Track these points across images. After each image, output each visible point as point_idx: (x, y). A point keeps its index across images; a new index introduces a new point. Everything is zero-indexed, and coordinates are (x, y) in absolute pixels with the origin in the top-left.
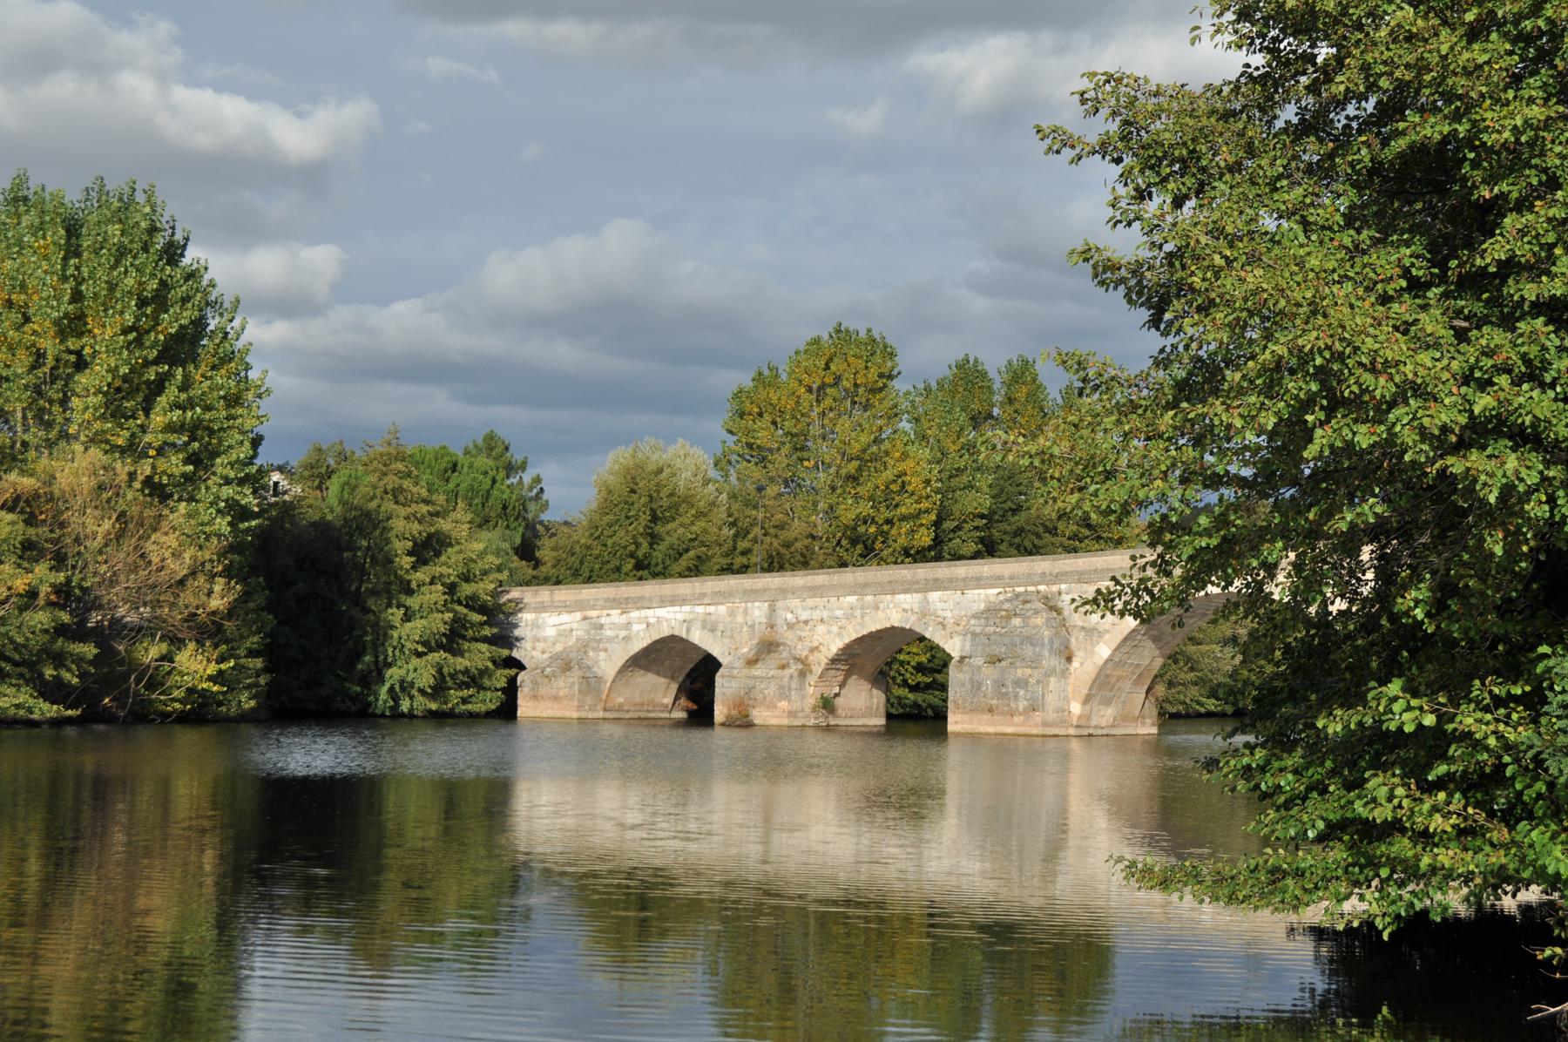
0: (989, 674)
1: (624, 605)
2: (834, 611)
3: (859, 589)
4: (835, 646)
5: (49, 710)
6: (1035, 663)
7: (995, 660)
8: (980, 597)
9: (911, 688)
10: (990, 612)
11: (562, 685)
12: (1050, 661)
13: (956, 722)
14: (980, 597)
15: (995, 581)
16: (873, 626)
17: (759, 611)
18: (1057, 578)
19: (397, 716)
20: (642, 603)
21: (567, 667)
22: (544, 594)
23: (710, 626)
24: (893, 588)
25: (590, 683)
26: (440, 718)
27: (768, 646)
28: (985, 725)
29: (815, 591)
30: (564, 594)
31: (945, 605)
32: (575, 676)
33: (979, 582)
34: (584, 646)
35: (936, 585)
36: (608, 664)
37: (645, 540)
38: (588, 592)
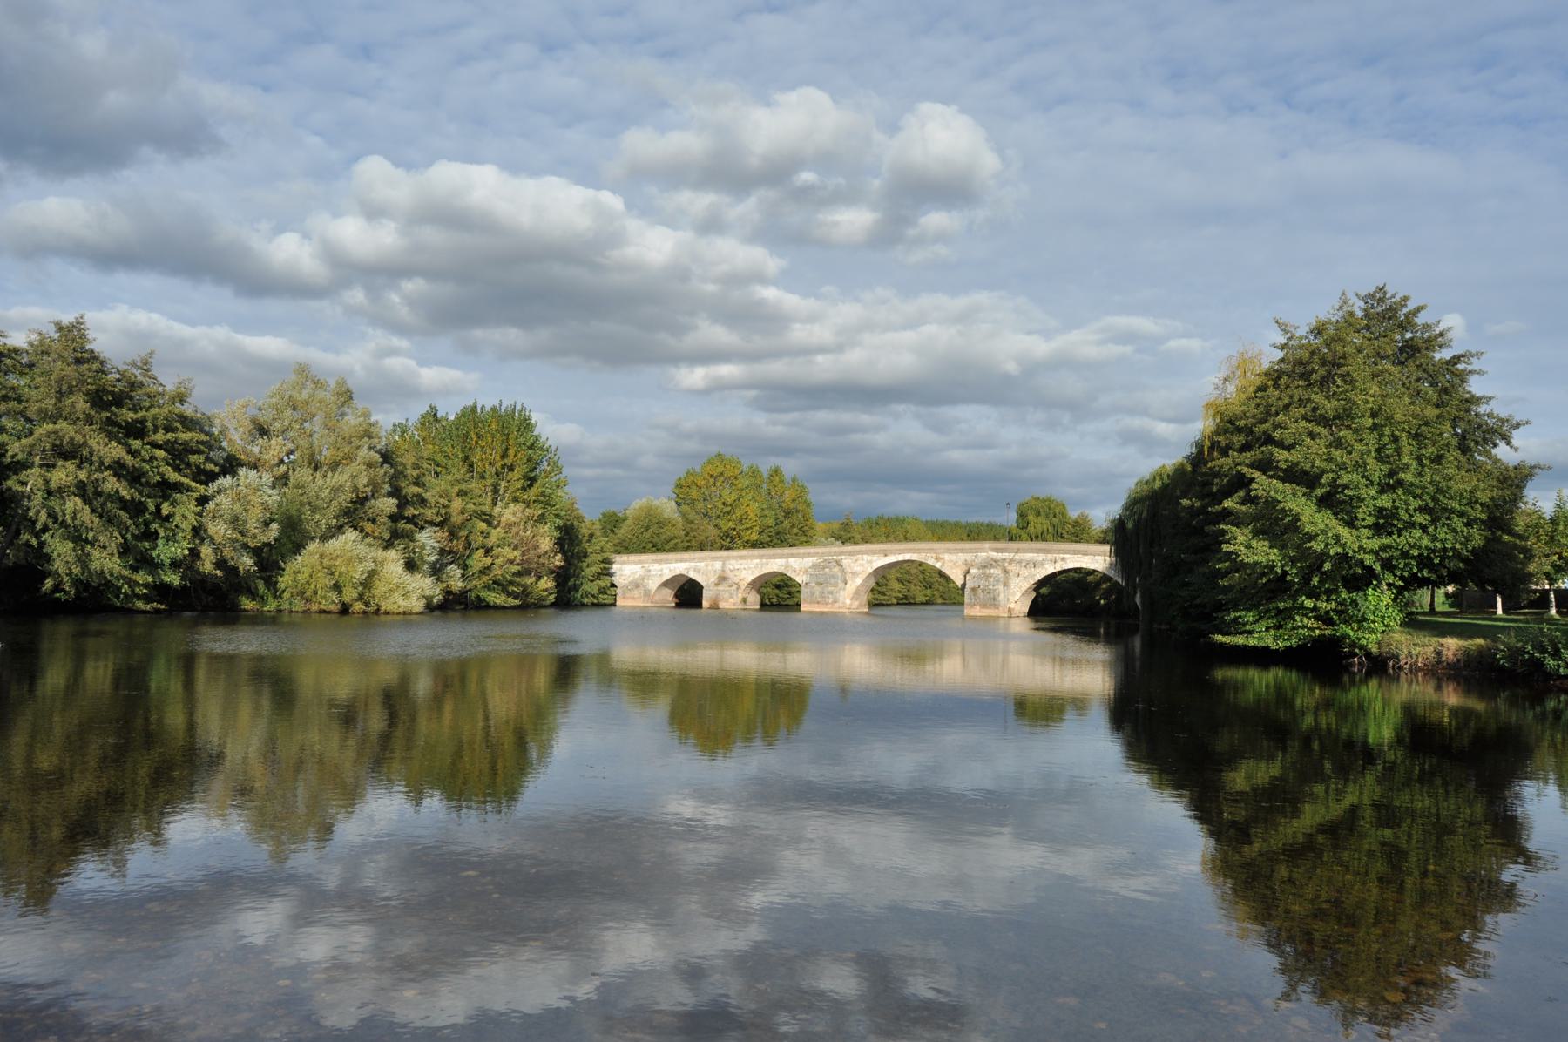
0: (817, 590)
1: (660, 562)
2: (748, 566)
3: (761, 557)
4: (750, 578)
5: (513, 602)
6: (836, 585)
7: (819, 584)
8: (809, 561)
9: (778, 596)
10: (814, 566)
11: (636, 593)
12: (841, 584)
13: (804, 607)
14: (809, 561)
15: (815, 554)
16: (766, 571)
17: (718, 565)
18: (841, 554)
19: (583, 605)
20: (667, 561)
21: (637, 586)
22: (625, 557)
23: (697, 571)
24: (774, 557)
25: (647, 593)
26: (594, 605)
27: (722, 579)
28: (817, 608)
29: (742, 558)
30: (633, 557)
31: (795, 564)
32: (641, 590)
33: (809, 555)
34: (643, 578)
35: (792, 556)
36: (653, 585)
37: (652, 538)
38: (644, 557)
